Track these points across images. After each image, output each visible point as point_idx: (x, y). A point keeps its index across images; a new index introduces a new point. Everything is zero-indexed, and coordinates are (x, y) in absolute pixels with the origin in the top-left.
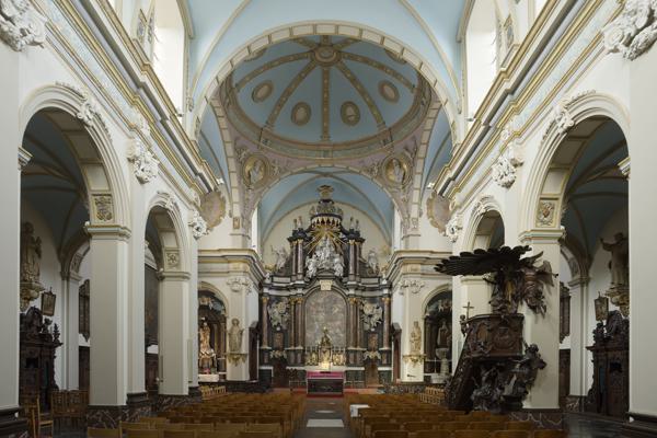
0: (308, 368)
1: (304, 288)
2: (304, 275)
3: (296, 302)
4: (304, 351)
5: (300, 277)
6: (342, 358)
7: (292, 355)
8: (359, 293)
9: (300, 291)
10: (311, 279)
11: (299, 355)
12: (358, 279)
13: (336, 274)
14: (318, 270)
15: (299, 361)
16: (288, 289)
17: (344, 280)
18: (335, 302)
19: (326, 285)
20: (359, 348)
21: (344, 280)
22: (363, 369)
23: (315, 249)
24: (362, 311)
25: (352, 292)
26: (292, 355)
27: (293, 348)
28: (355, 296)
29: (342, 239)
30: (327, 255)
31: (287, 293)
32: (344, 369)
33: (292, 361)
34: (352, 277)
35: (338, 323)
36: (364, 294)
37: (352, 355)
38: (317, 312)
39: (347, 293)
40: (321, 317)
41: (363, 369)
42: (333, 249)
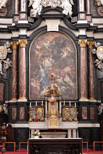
0: (32, 125)
1: (28, 30)
2: (28, 12)
3: (18, 47)
4: (28, 104)
5: (23, 16)
6: (74, 112)
7: (14, 110)
8: (90, 34)
9: (23, 32)
10: (35, 19)
11: (22, 110)
12: (89, 18)
13: (64, 12)
15: (22, 116)
16: (9, 30)
17: (74, 19)
18: (64, 45)
19: (53, 25)
20: (93, 100)
21: (74, 19)
22: (98, 125)
24: (95, 56)
25: (82, 32)
26: (14, 110)
27: (13, 101)
28: (85, 37)
31: (8, 36)
32: (75, 125)
33: (14, 117)
34: (82, 16)
35: (67, 69)
36: (97, 36)
37: (84, 109)
38: (43, 57)
39: (77, 34)
40: (48, 62)
41: (98, 125)
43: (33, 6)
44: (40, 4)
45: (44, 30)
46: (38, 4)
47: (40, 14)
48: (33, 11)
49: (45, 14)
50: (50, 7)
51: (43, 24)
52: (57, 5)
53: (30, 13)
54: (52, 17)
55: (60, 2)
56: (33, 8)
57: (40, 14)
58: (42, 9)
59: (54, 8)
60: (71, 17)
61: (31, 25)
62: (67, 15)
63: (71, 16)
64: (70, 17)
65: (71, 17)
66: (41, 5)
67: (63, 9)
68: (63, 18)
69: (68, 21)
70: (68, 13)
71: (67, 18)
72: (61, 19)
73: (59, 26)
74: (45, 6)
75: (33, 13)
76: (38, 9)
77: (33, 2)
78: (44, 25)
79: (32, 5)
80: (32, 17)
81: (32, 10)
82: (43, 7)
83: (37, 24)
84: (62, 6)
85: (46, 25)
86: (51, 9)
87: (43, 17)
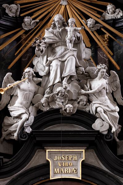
10: (16, 144)
13: (97, 125)
14: (40, 114)
19: (67, 163)
23: (32, 53)
29: (113, 22)
30: (70, 69)
42: (86, 53)
43: (10, 108)
44: (31, 102)
45: (40, 176)
46: (24, 102)
47: (31, 130)
48: (9, 122)
49: (44, 130)
50: (58, 111)
51: (35, 161)
52: (77, 105)
53: (2, 127)
54: (61, 139)
55: (84, 98)
56: (12, 114)
57: (28, 130)
58: (35, 118)
59: (68, 116)
60: (117, 140)
61: (5, 160)
62: (106, 133)
63: (116, 138)
64: (114, 140)
65: (117, 140)
66: (33, 105)
67: (93, 118)
68: (94, 141)
69: (109, 151)
70: (108, 127)
71: (107, 142)
72: (88, 145)
73: (84, 165)
74: (46, 109)
75: (12, 129)
76: (24, 117)
77: (11, 97)
78: (42, 162)
79: (7, 105)
80: (7, 138)
81: (7, 121)
82: (39, 111)
83: (22, 159)
84: (92, 108)
85: (48, 161)
86: (61, 116)
87: (38, 139)
